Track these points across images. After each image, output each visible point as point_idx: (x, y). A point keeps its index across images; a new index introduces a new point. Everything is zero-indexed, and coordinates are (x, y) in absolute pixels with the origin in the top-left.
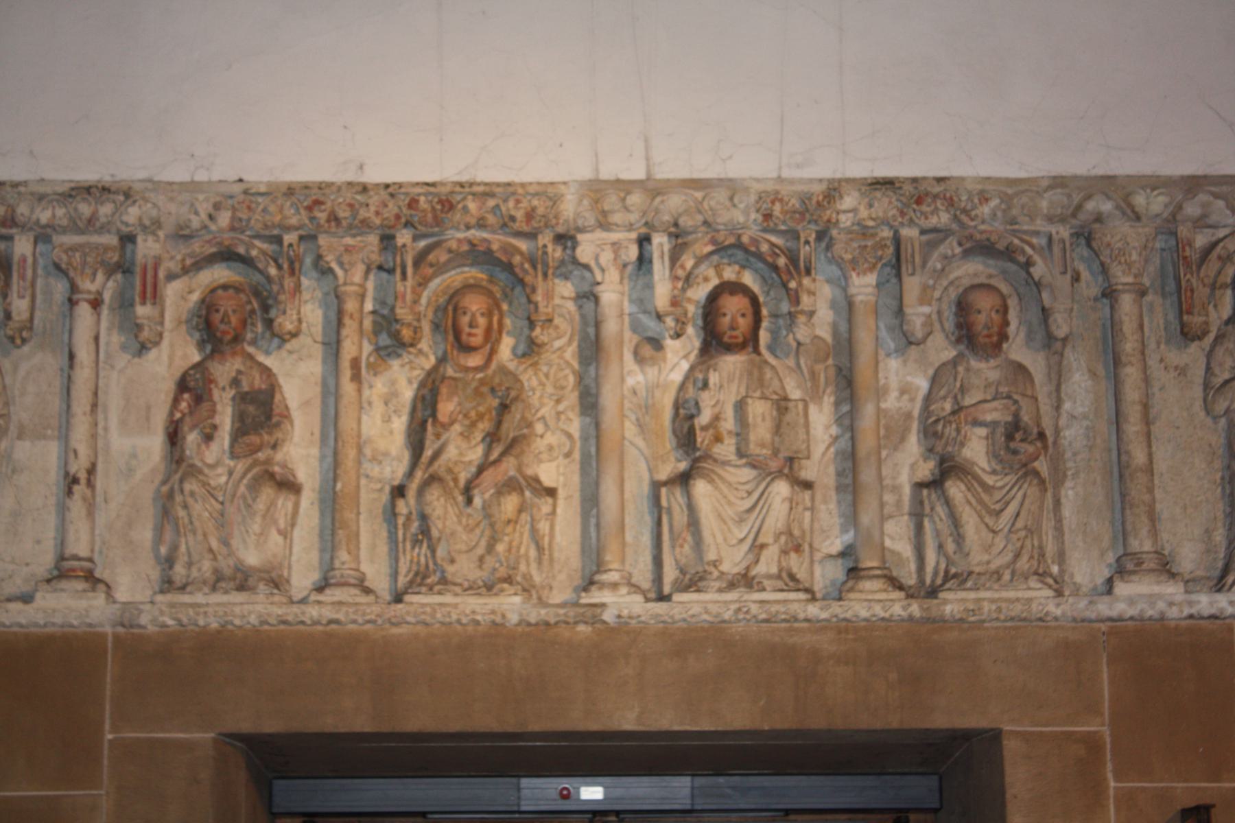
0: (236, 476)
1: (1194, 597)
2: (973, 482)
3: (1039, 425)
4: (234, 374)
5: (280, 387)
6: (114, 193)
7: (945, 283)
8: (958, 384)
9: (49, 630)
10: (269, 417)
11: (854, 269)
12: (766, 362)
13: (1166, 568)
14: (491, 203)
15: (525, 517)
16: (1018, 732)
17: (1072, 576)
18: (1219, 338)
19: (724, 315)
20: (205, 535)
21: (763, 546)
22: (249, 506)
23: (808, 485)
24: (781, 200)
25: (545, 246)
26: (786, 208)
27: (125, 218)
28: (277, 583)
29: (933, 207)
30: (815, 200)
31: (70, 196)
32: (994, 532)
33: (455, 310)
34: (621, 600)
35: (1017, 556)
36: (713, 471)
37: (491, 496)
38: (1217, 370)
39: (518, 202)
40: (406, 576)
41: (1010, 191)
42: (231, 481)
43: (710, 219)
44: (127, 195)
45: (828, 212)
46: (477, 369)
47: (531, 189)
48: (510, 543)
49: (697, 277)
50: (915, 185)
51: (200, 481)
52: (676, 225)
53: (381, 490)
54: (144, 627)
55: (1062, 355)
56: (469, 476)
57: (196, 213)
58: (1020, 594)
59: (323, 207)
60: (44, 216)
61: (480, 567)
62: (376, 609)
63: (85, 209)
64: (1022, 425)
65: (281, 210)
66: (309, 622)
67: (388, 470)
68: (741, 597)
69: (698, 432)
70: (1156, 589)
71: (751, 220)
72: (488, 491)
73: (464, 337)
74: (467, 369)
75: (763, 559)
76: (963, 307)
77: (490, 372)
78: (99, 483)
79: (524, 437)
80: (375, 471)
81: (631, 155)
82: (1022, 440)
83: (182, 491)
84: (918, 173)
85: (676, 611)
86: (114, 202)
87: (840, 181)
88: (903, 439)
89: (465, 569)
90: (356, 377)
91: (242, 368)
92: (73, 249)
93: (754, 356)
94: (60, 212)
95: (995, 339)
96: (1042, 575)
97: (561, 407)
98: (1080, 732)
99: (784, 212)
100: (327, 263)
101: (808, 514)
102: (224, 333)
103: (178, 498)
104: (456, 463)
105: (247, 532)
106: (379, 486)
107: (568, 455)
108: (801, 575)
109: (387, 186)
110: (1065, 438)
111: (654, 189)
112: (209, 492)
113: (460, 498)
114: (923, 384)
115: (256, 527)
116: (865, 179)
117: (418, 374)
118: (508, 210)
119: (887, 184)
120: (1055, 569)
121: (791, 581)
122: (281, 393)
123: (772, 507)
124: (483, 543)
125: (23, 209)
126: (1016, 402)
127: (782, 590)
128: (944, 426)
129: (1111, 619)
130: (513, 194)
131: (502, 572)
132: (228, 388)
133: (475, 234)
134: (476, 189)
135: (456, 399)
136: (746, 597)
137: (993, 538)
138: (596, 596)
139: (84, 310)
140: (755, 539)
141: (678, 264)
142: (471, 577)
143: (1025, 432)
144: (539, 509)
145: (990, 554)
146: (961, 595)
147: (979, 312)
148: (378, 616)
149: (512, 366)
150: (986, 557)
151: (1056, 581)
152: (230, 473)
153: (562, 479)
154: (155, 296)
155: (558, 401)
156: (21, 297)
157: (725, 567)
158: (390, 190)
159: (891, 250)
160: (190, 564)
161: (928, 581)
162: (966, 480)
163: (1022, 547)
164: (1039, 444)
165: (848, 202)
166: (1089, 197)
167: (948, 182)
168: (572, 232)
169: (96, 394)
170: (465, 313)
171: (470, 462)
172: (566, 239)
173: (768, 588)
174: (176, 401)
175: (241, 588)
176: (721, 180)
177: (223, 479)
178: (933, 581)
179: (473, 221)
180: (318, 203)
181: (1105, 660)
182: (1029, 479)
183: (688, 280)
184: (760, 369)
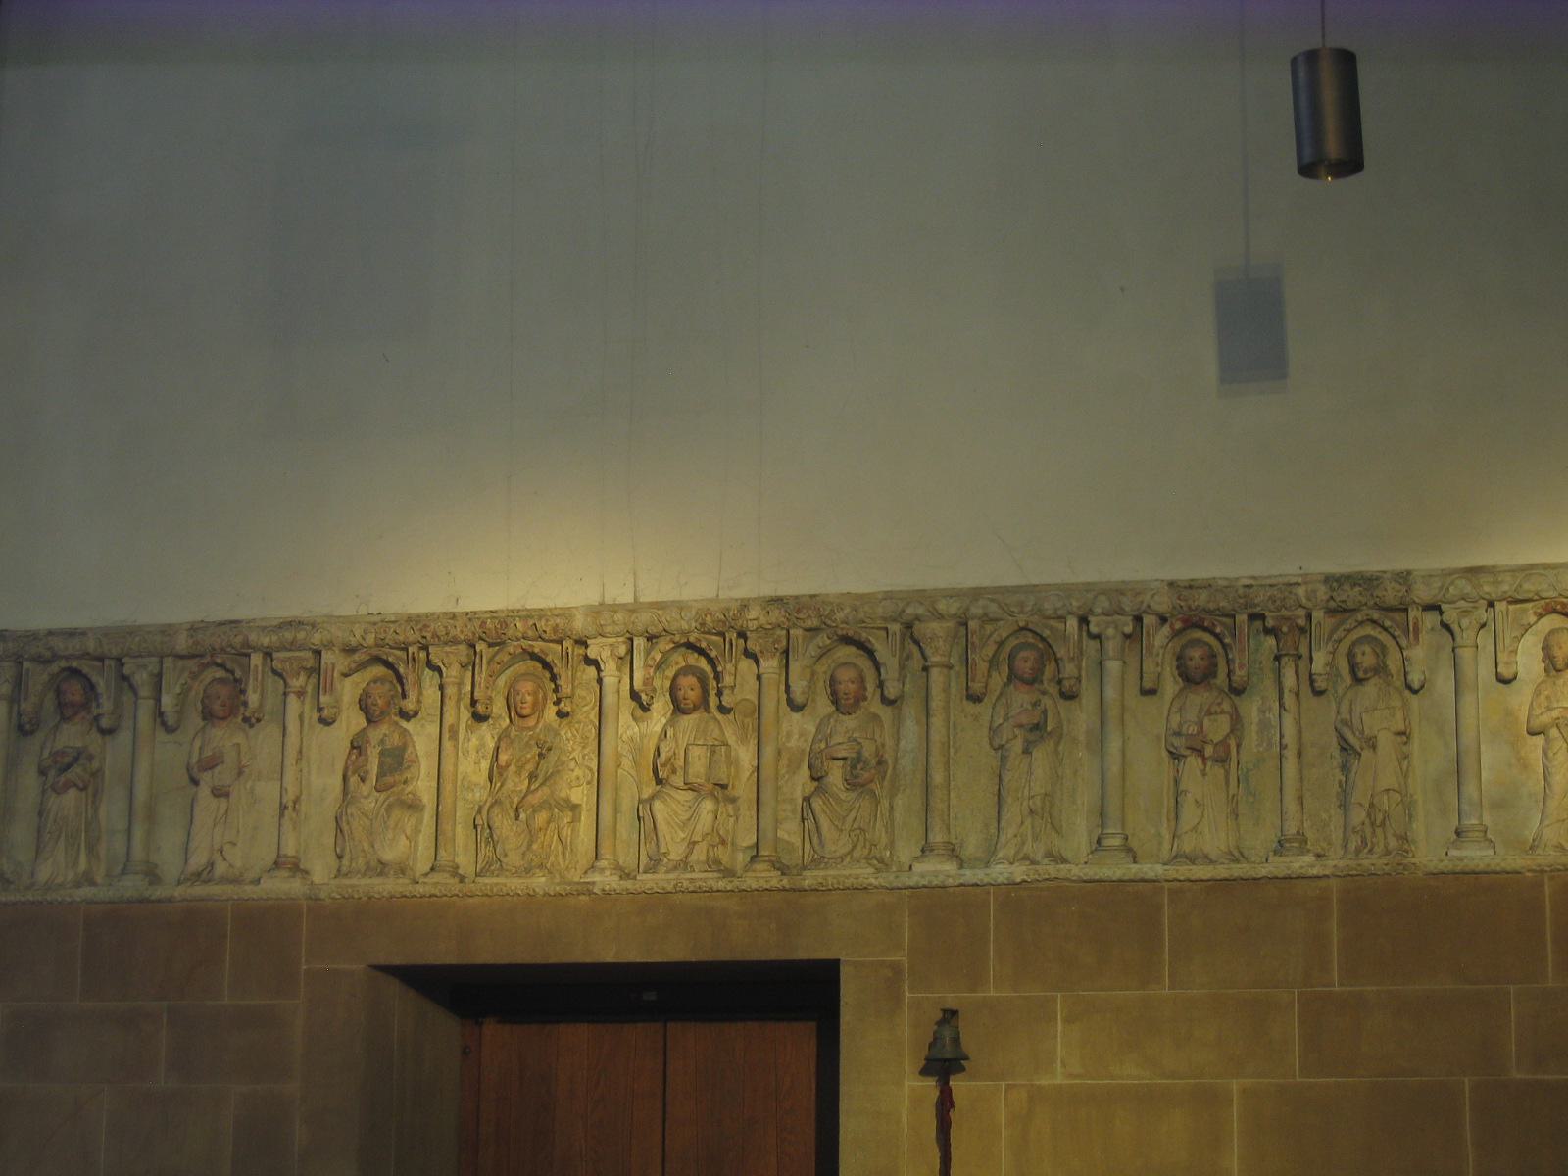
1: (962, 872)
4: (381, 737)
8: (829, 731)
9: (270, 902)
10: (400, 764)
13: (953, 852)
14: (531, 623)
15: (552, 826)
17: (898, 857)
18: (1001, 694)
21: (695, 843)
22: (385, 823)
23: (733, 800)
24: (711, 614)
30: (731, 614)
31: (280, 628)
32: (841, 830)
35: (854, 847)
38: (995, 719)
39: (547, 621)
41: (858, 603)
44: (313, 626)
45: (741, 622)
46: (529, 729)
47: (555, 612)
54: (324, 899)
60: (265, 641)
61: (523, 859)
63: (288, 635)
64: (864, 758)
67: (478, 794)
70: (939, 867)
76: (833, 682)
77: (538, 730)
78: (303, 807)
80: (470, 796)
82: (862, 769)
86: (305, 630)
87: (749, 599)
89: (514, 859)
91: (387, 732)
92: (283, 661)
94: (275, 638)
95: (851, 701)
99: (714, 622)
102: (375, 710)
108: (725, 860)
109: (467, 614)
111: (633, 609)
113: (512, 815)
114: (812, 729)
115: (390, 835)
116: (765, 597)
119: (778, 600)
121: (714, 864)
122: (414, 746)
124: (525, 844)
125: (253, 637)
126: (860, 743)
127: (706, 871)
130: (544, 616)
131: (537, 861)
133: (525, 643)
134: (521, 613)
136: (682, 876)
139: (292, 700)
142: (518, 865)
143: (865, 763)
144: (563, 821)
146: (816, 873)
147: (840, 683)
149: (555, 725)
153: (585, 798)
155: (584, 747)
156: (255, 692)
159: (784, 643)
160: (351, 860)
163: (858, 840)
165: (753, 614)
166: (908, 604)
168: (585, 639)
169: (300, 752)
171: (521, 791)
172: (582, 642)
175: (381, 874)
176: (673, 601)
177: (373, 804)
179: (521, 635)
180: (425, 626)
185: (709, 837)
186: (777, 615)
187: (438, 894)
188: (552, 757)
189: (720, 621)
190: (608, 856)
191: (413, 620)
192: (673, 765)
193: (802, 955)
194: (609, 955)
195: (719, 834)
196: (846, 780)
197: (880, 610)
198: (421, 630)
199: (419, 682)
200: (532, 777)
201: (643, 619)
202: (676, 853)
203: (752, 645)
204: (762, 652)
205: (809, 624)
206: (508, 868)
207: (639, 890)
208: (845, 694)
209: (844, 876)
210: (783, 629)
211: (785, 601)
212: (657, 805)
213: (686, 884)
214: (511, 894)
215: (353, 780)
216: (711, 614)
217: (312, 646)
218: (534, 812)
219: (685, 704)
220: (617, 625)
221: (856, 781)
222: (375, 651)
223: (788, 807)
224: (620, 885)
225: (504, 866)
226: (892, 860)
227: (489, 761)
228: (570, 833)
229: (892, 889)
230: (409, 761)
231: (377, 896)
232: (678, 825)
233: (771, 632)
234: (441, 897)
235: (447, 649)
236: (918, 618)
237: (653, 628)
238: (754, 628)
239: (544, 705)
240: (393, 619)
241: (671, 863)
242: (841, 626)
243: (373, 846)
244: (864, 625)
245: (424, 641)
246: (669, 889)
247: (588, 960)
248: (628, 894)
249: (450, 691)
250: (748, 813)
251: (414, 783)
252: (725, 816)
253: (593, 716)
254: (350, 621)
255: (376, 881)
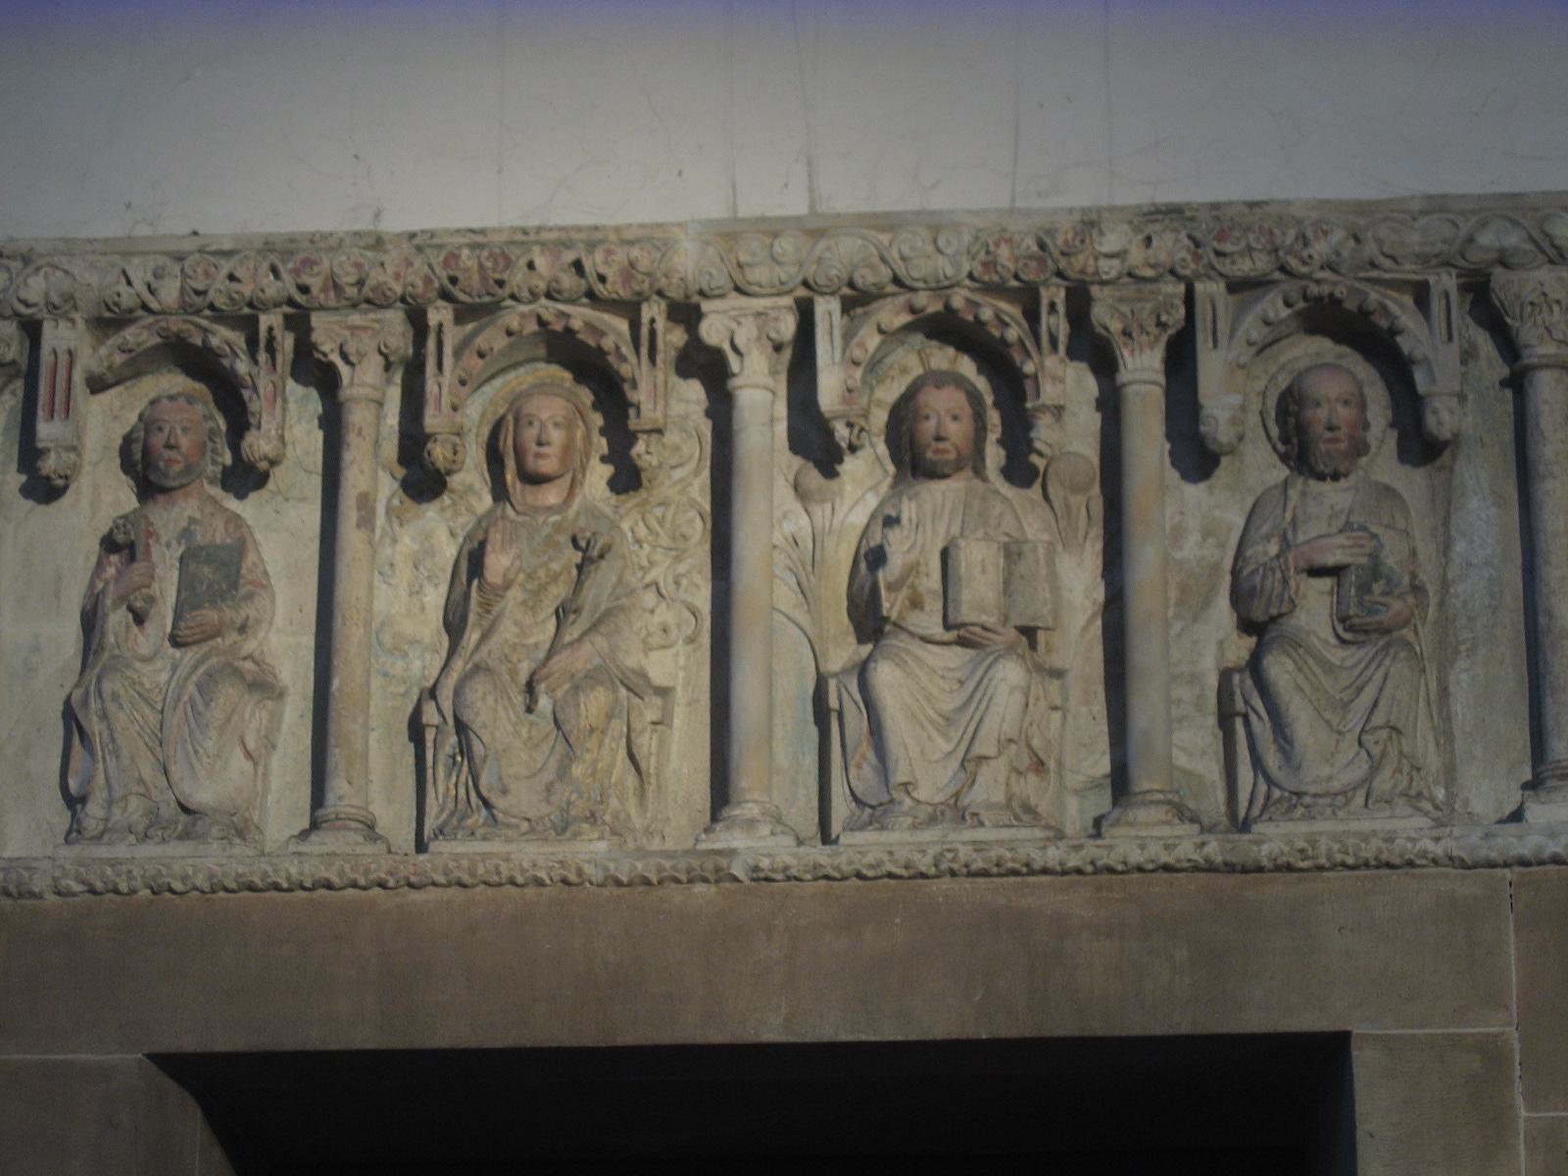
0: (182, 672)
2: (1307, 657)
3: (1414, 576)
4: (184, 524)
5: (256, 544)
6: (8, 257)
7: (1273, 369)
8: (1288, 516)
10: (234, 585)
11: (1125, 345)
12: (996, 492)
14: (569, 256)
16: (1376, 1037)
17: (1466, 802)
19: (927, 418)
20: (132, 759)
22: (197, 714)
23: (1058, 674)
24: (1009, 241)
25: (653, 321)
26: (1016, 252)
27: (23, 294)
28: (240, 829)
29: (1243, 245)
30: (1060, 241)
32: (1340, 733)
33: (517, 420)
34: (761, 844)
36: (906, 651)
37: (567, 692)
39: (609, 252)
40: (437, 817)
41: (1362, 222)
42: (175, 678)
43: (902, 272)
44: (26, 260)
45: (1081, 257)
46: (551, 510)
47: (629, 235)
48: (594, 763)
49: (891, 367)
50: (1214, 213)
51: (127, 678)
52: (851, 284)
53: (404, 695)
54: (39, 896)
55: (1451, 470)
56: (533, 666)
57: (129, 283)
58: (1378, 825)
59: (316, 269)
61: (548, 801)
62: (386, 863)
65: (254, 276)
66: (285, 885)
67: (417, 665)
68: (945, 836)
69: (883, 592)
71: (965, 273)
72: (560, 686)
73: (531, 463)
74: (537, 509)
75: (980, 780)
77: (571, 513)
79: (622, 608)
81: (786, 185)
82: (1387, 593)
83: (100, 693)
84: (1221, 196)
85: (843, 859)
86: (8, 269)
87: (1099, 210)
88: (1207, 603)
89: (523, 799)
90: (366, 521)
91: (198, 516)
93: (977, 483)
95: (1343, 446)
96: (1413, 798)
97: (682, 568)
98: (1473, 1035)
100: (325, 355)
101: (1056, 716)
102: (170, 461)
103: (94, 705)
104: (514, 647)
105: (196, 752)
106: (402, 689)
107: (691, 640)
109: (412, 236)
110: (1457, 596)
111: (816, 230)
112: (140, 695)
113: (519, 700)
115: (210, 745)
116: (1139, 207)
117: (465, 522)
118: (595, 265)
119: (1173, 213)
120: (1440, 794)
123: (995, 700)
124: (553, 765)
126: (1375, 536)
127: (1006, 826)
128: (1264, 577)
129: (1524, 862)
131: (580, 807)
132: (174, 542)
133: (547, 308)
134: (545, 236)
135: (514, 550)
136: (952, 836)
137: (1338, 742)
138: (722, 840)
140: (967, 751)
141: (855, 341)
143: (1389, 581)
144: (641, 714)
145: (1332, 766)
147: (1318, 404)
148: (390, 873)
149: (608, 511)
150: (1326, 771)
151: (1436, 807)
152: (174, 669)
153: (681, 674)
154: (67, 412)
155: (678, 559)
157: (922, 794)
158: (417, 241)
159: (1181, 312)
160: (110, 803)
161: (1242, 813)
162: (1294, 654)
163: (1384, 754)
164: (1410, 600)
165: (1111, 242)
166: (1483, 224)
167: (1266, 208)
170: (531, 424)
171: (536, 646)
172: (686, 313)
173: (987, 823)
174: (100, 566)
175: (185, 836)
176: (919, 213)
177: (164, 677)
178: (1249, 809)
179: (542, 286)
180: (309, 263)
181: (1511, 925)
182: (1392, 651)
183: (874, 367)
184: (984, 499)
185: (1013, 747)
186: (1170, 246)
187: (336, 880)
188: (604, 577)
189: (1031, 257)
190: (756, 795)
191: (277, 252)
192: (913, 587)
193: (1255, 1020)
194: (770, 1027)
195: (1029, 746)
196: (1343, 620)
197: (1414, 238)
198: (296, 272)
199: (279, 393)
200: (564, 613)
201: (844, 255)
202: (932, 784)
203: (1105, 315)
204: (1127, 333)
205: (1244, 267)
206: (514, 821)
207: (847, 869)
208: (1330, 428)
209: (1357, 834)
210: (1179, 278)
211: (1188, 214)
212: (884, 674)
213: (965, 853)
214: (520, 880)
215: (117, 619)
216: (1009, 241)
217: (22, 310)
218: (576, 688)
219: (937, 451)
220: (778, 263)
221: (1377, 618)
222: (176, 324)
223: (1183, 692)
224: (795, 856)
225: (500, 816)
226: (1453, 810)
227: (444, 588)
228: (654, 750)
229: (1475, 866)
230: (251, 583)
231: (178, 886)
232: (932, 722)
233: (1149, 287)
234: (341, 889)
235: (356, 319)
236: (1503, 261)
237: (867, 272)
238: (1113, 274)
239: (587, 455)
240: (227, 246)
241: (923, 807)
242: (1321, 275)
243: (166, 772)
244: (1374, 274)
245: (300, 298)
246: (923, 869)
247: (717, 1037)
248: (816, 879)
249: (358, 416)
250: (1084, 709)
251: (261, 635)
252: (1043, 705)
253: (700, 489)
254: (127, 249)
255: (177, 849)
